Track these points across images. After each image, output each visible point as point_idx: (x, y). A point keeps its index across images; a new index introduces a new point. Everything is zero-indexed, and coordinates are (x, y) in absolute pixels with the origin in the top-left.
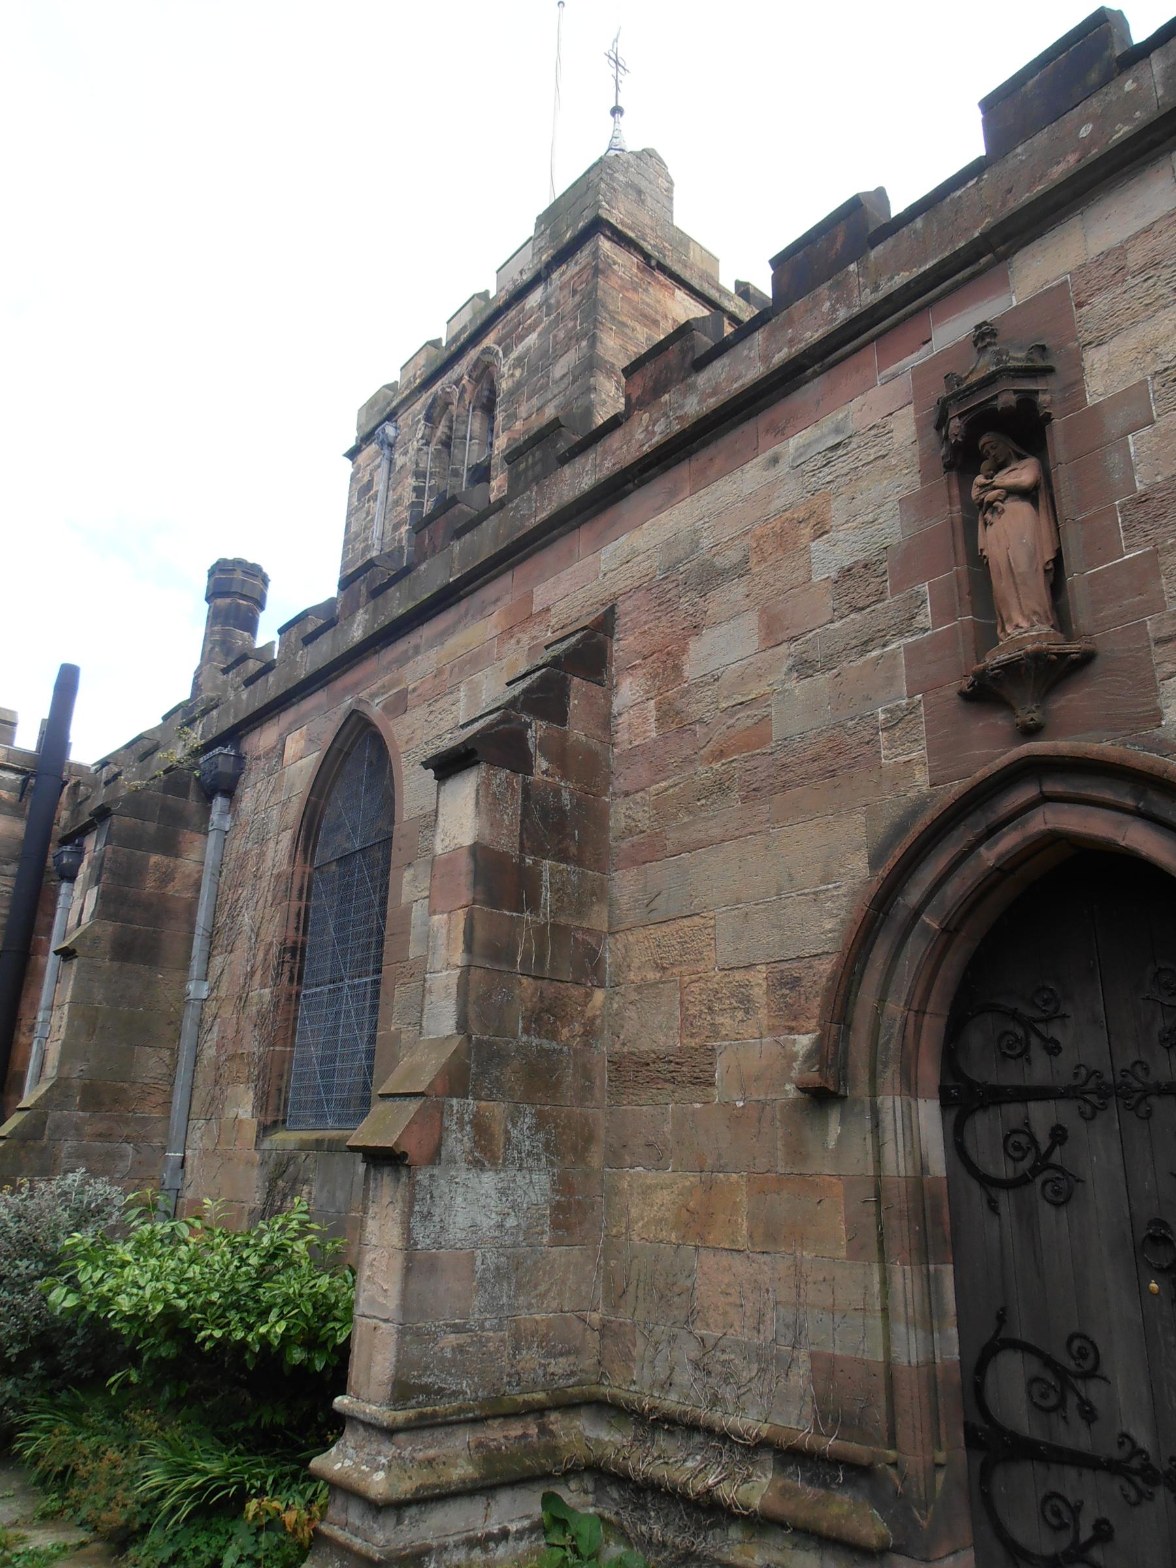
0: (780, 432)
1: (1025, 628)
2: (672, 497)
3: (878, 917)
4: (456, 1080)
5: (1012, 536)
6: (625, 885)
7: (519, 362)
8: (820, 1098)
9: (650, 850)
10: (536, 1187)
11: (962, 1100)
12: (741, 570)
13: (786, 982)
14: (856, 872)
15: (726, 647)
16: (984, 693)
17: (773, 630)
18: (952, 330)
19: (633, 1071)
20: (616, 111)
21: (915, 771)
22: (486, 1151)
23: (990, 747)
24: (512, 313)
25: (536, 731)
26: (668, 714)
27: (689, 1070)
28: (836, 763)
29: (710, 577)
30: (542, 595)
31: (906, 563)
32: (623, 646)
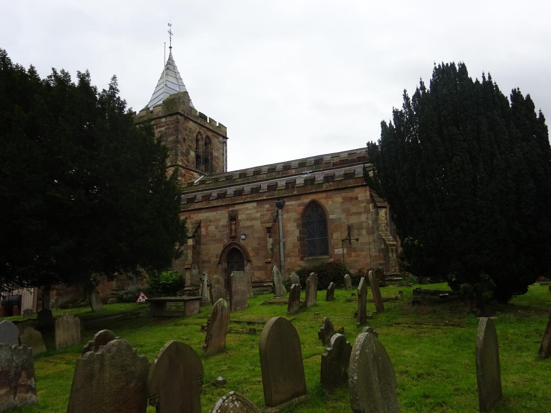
0: (217, 211)
1: (233, 234)
2: (207, 212)
3: (224, 251)
4: (193, 263)
5: (233, 227)
6: (203, 247)
7: (160, 132)
8: (219, 263)
9: (205, 244)
10: (197, 271)
11: (228, 263)
12: (213, 222)
13: (217, 255)
14: (222, 248)
15: (212, 228)
16: (231, 238)
17: (216, 228)
18: (231, 209)
19: (204, 262)
20: (171, 48)
21: (226, 241)
22: (194, 268)
23: (231, 241)
24: (157, 120)
25: (196, 234)
26: (207, 232)
27: (209, 262)
28: (221, 240)
29: (210, 221)
30: (192, 216)
31: (226, 226)
32: (202, 225)
